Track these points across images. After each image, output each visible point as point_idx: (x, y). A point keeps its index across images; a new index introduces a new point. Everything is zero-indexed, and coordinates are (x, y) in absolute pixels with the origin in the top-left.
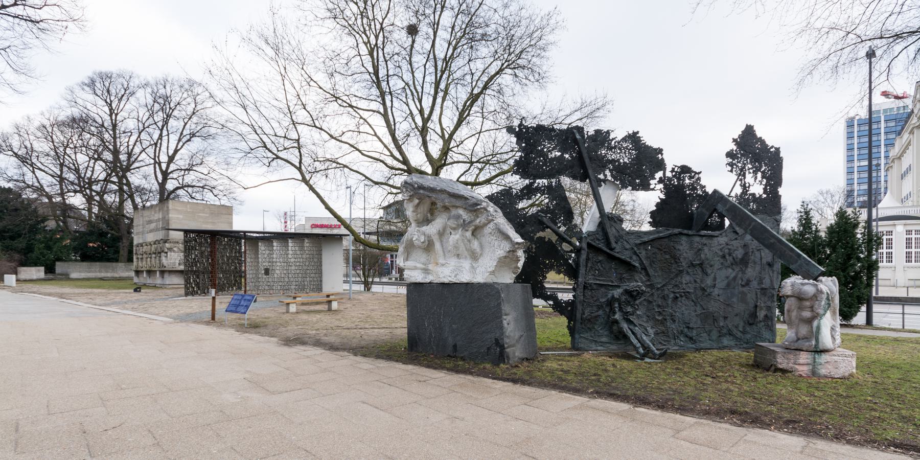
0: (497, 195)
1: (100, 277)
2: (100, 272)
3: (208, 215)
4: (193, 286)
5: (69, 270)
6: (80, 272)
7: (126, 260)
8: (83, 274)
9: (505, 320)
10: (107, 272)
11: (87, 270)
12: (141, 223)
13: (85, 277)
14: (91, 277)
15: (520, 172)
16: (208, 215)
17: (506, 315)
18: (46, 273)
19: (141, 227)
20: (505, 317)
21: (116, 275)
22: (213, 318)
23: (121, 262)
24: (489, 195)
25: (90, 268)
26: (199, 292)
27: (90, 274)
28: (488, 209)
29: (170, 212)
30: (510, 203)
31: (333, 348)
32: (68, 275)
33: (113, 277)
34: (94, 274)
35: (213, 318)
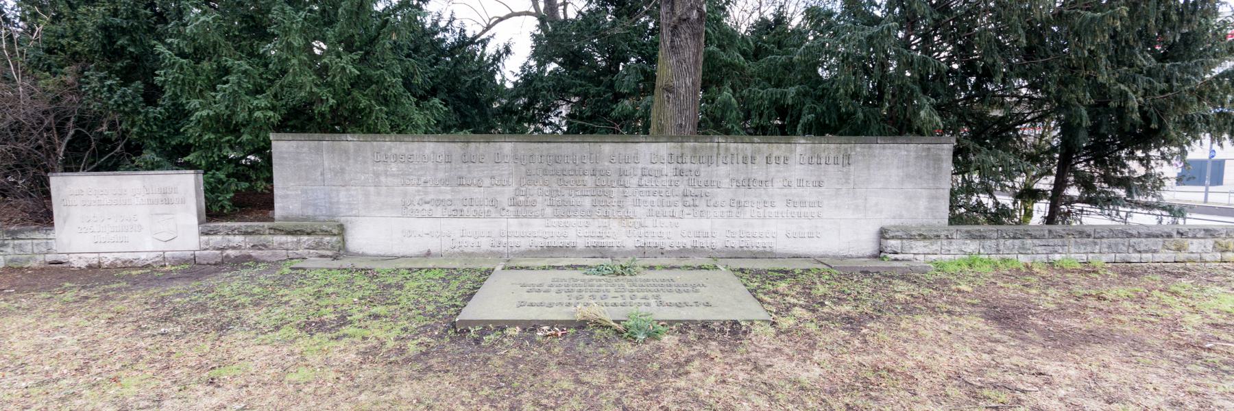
2: (522, 207)
5: (343, 196)
6: (405, 208)
7: (693, 114)
8: (423, 225)
10: (564, 210)
11: (446, 193)
13: (434, 245)
14: (469, 245)
18: (213, 212)
21: (620, 236)
23: (662, 135)
25: (461, 182)
27: (461, 223)
32: (342, 229)
33: (600, 251)
34: (482, 225)
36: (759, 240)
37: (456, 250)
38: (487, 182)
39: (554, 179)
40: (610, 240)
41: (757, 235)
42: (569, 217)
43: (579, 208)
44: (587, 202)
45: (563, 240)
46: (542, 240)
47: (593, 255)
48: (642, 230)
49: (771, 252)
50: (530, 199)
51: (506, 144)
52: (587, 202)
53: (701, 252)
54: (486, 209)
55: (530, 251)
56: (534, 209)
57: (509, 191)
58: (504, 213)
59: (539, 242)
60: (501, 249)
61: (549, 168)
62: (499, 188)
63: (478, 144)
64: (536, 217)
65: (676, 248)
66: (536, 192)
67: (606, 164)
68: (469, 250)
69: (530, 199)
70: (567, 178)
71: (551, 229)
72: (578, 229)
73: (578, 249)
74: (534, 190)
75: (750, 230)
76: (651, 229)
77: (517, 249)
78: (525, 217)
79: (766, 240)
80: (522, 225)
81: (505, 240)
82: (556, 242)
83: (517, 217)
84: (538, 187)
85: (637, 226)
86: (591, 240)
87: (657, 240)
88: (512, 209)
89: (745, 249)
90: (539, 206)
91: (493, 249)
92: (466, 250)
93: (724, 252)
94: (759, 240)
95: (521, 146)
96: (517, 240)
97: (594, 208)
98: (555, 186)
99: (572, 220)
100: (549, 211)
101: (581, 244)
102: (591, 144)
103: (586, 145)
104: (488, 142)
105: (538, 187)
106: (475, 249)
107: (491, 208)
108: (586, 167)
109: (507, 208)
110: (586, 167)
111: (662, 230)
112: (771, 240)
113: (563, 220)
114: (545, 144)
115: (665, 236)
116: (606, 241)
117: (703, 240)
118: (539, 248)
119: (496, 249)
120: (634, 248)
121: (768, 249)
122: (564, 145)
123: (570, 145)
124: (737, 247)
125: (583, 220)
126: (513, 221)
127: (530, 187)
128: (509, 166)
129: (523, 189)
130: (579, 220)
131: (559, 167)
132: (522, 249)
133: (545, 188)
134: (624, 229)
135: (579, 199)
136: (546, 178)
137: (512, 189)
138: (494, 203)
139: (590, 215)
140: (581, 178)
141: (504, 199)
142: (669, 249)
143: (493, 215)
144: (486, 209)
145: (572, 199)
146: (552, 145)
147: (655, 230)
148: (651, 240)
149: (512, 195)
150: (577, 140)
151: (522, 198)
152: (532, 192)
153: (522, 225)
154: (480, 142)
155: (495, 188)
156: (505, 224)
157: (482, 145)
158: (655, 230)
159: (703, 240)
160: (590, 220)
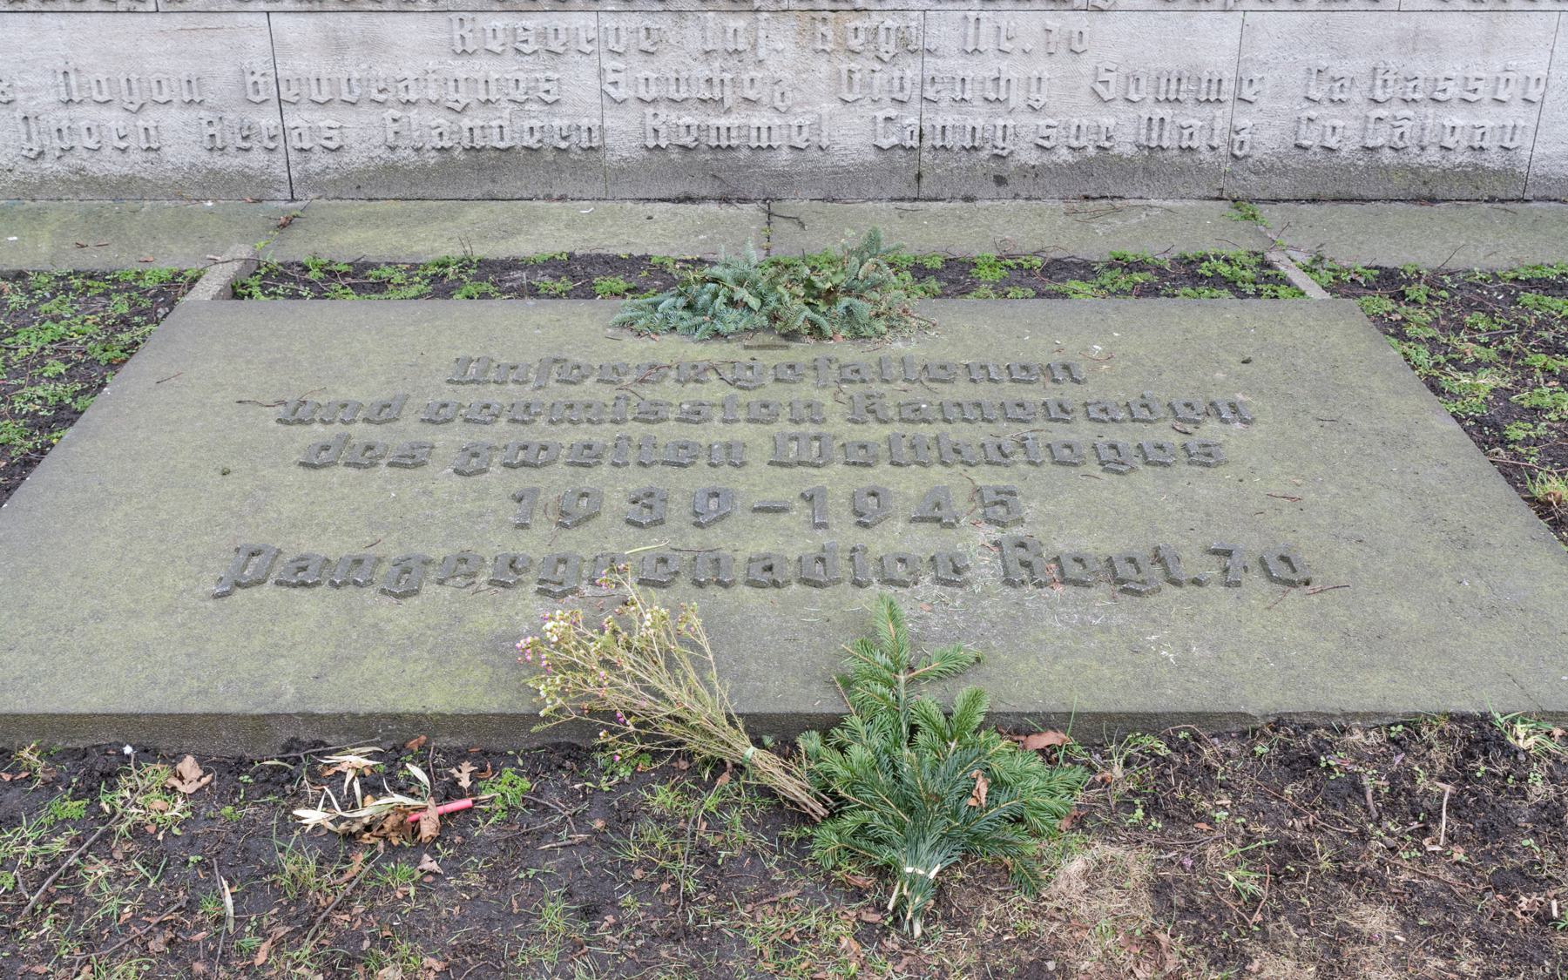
36: (1459, 118)
37: (48, 165)
40: (760, 119)
41: (1453, 90)
45: (537, 117)
46: (442, 120)
47: (679, 189)
48: (911, 70)
49: (1506, 174)
53: (1181, 171)
55: (392, 169)
60: (257, 159)
65: (1064, 155)
68: (110, 166)
71: (482, 67)
72: (610, 63)
73: (611, 158)
75: (1421, 67)
76: (952, 64)
77: (329, 160)
79: (1489, 118)
81: (267, 120)
85: (888, 47)
87: (979, 118)
89: (1387, 157)
91: (219, 161)
92: (94, 168)
93: (1284, 172)
94: (1459, 118)
96: (324, 119)
99: (579, 22)
106: (134, 164)
111: (1010, 69)
112: (1515, 114)
113: (534, 22)
115: (1017, 99)
116: (733, 123)
117: (1193, 118)
118: (432, 158)
119: (233, 162)
120: (872, 157)
121: (1494, 160)
124: (1348, 148)
130: (610, 22)
132: (356, 158)
134: (823, 67)
142: (1032, 158)
147: (976, 70)
148: (950, 119)
153: (338, 46)
156: (260, 43)
158: (976, 70)
159: (1193, 118)
160: (664, 22)
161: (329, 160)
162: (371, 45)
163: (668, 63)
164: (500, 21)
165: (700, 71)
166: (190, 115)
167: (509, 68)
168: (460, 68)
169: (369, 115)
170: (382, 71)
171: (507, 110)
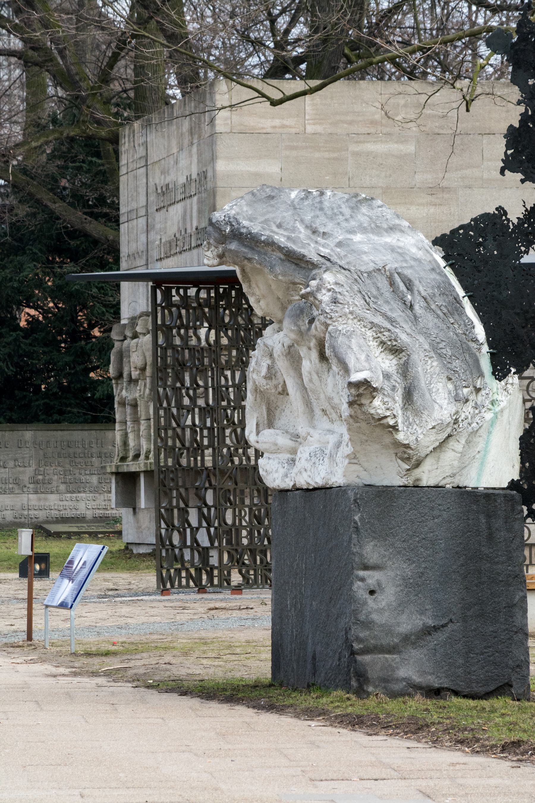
0: (466, 233)
1: (42, 515)
3: (410, 148)
4: (203, 539)
9: (363, 580)
12: (142, 201)
15: (521, 162)
16: (410, 148)
17: (366, 568)
19: (142, 222)
20: (361, 573)
22: (30, 637)
24: (444, 235)
26: (236, 578)
28: (319, 296)
29: (221, 148)
30: (501, 255)
31: (184, 692)
35: (30, 637)
38: (11, 464)
39: (67, 460)
42: (79, 492)
43: (88, 485)
44: (94, 480)
45: (74, 512)
46: (57, 512)
50: (47, 478)
51: (27, 432)
52: (94, 480)
54: (11, 486)
56: (50, 486)
57: (29, 471)
58: (25, 489)
59: (55, 514)
60: (23, 520)
61: (63, 452)
62: (22, 469)
63: (4, 433)
64: (52, 493)
66: (52, 471)
67: (110, 447)
69: (47, 478)
70: (78, 460)
71: (65, 503)
72: (88, 502)
74: (50, 470)
77: (36, 520)
78: (42, 493)
80: (40, 500)
81: (26, 513)
82: (69, 514)
83: (36, 492)
84: (54, 467)
86: (98, 511)
88: (32, 486)
90: (55, 484)
91: (16, 520)
95: (39, 433)
96: (36, 512)
97: (100, 485)
98: (68, 466)
99: (83, 495)
100: (62, 487)
101: (89, 514)
102: (98, 432)
103: (93, 432)
104: (13, 431)
105: (54, 467)
107: (15, 486)
108: (94, 450)
109: (28, 485)
110: (94, 450)
113: (75, 495)
114: (60, 433)
118: (55, 519)
122: (75, 433)
123: (80, 432)
125: (91, 495)
126: (31, 496)
127: (47, 468)
128: (30, 450)
129: (41, 469)
130: (88, 495)
131: (71, 450)
132: (41, 519)
133: (59, 468)
135: (88, 477)
136: (60, 460)
137: (32, 469)
138: (17, 482)
139: (96, 490)
140: (89, 460)
141: (25, 478)
143: (17, 492)
144: (11, 486)
145: (82, 478)
146: (66, 433)
149: (32, 474)
150: (86, 428)
151: (40, 477)
152: (48, 472)
154: (5, 431)
155: (18, 469)
156: (26, 499)
157: (7, 434)
160: (97, 495)
161: (36, 520)
162: (46, 499)
163: (97, 502)
164: (69, 495)
165: (104, 503)
166: (12, 512)
167: (70, 503)
168: (61, 503)
169: (44, 512)
170: (47, 504)
171: (69, 510)
